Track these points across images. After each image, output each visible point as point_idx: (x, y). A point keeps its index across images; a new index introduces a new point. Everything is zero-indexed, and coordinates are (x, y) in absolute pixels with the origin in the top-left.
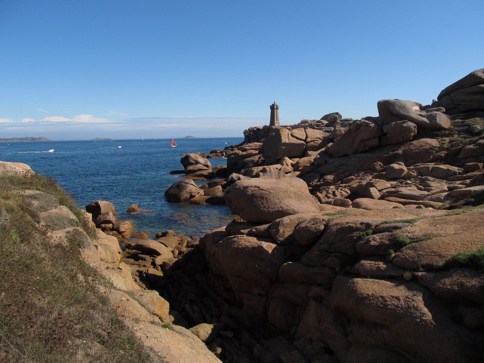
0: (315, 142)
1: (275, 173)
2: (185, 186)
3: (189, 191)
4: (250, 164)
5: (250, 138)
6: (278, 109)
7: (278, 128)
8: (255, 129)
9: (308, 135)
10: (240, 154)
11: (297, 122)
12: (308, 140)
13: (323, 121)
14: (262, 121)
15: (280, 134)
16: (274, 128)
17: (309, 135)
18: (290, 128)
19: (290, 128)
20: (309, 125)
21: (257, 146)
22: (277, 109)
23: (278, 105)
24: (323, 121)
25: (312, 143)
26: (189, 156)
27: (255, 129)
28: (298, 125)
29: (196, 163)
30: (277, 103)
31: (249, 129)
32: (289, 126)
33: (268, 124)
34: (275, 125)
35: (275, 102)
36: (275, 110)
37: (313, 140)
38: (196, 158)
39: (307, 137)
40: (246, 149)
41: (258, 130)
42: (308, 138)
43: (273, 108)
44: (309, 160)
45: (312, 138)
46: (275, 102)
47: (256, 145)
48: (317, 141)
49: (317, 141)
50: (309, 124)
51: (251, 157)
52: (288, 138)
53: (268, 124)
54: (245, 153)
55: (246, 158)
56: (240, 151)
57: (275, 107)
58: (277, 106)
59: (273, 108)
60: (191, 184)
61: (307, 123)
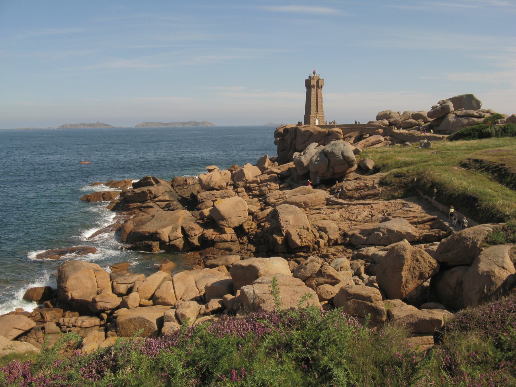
6: (322, 86)
7: (312, 131)
8: (281, 130)
11: (367, 115)
18: (340, 130)
19: (340, 130)
23: (321, 78)
27: (281, 130)
32: (339, 126)
34: (311, 123)
35: (314, 73)
36: (313, 91)
43: (312, 86)
46: (314, 73)
57: (313, 83)
58: (318, 82)
59: (312, 86)
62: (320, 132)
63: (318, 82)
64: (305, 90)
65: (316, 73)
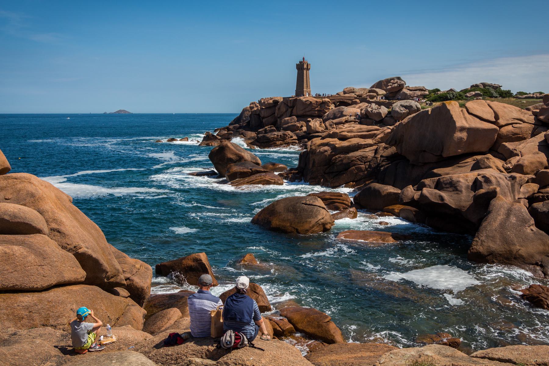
0: (514, 125)
1: (507, 186)
2: (312, 211)
3: (322, 221)
4: (359, 163)
5: (262, 116)
8: (271, 101)
9: (498, 113)
10: (337, 146)
12: (502, 122)
13: (377, 90)
14: (284, 90)
15: (449, 110)
16: (304, 100)
17: (500, 114)
20: (358, 96)
21: (363, 131)
22: (308, 69)
24: (377, 90)
25: (510, 128)
26: (227, 146)
28: (335, 96)
29: (238, 158)
30: (308, 60)
31: (260, 102)
33: (294, 94)
35: (304, 59)
36: (305, 72)
37: (510, 122)
38: (237, 150)
39: (497, 117)
40: (345, 135)
41: (276, 102)
42: (499, 119)
43: (302, 68)
44: (538, 160)
45: (508, 118)
46: (304, 59)
47: (361, 129)
48: (516, 123)
49: (516, 123)
50: (357, 94)
51: (357, 150)
52: (465, 118)
53: (291, 93)
54: (345, 144)
55: (348, 153)
56: (336, 139)
57: (305, 66)
59: (302, 68)
60: (320, 207)
61: (353, 92)
62: (316, 102)
63: (307, 66)
64: (296, 71)
65: (305, 59)
